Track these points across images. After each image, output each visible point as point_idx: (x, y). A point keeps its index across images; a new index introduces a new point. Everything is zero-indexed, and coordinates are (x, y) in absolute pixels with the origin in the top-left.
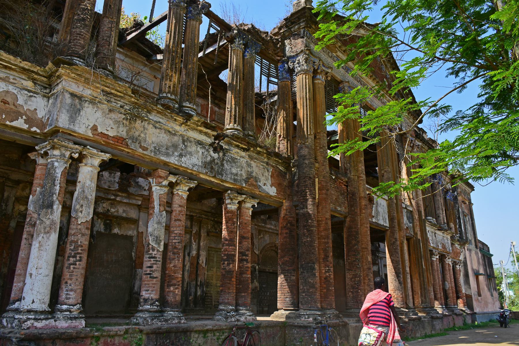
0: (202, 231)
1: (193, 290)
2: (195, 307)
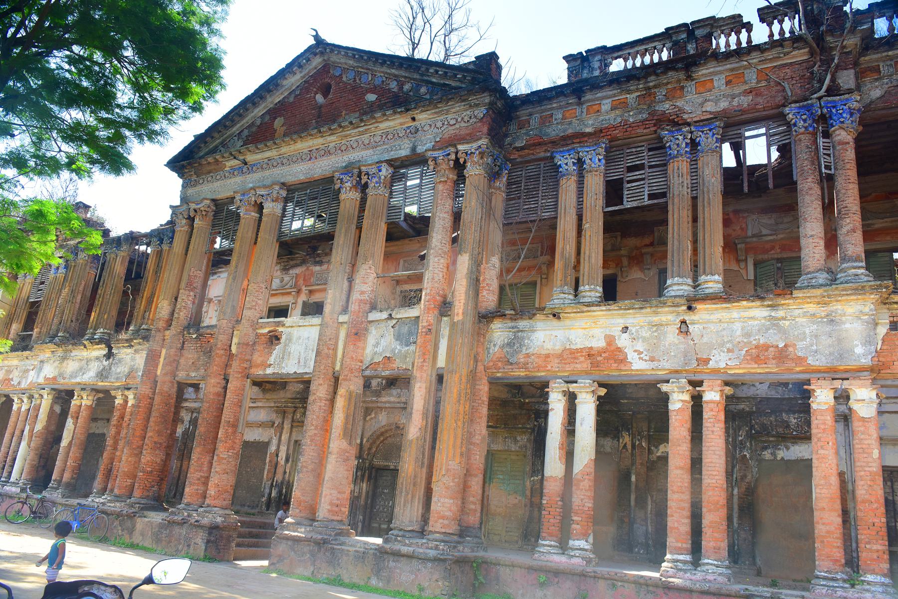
1: (267, 491)
2: (268, 510)
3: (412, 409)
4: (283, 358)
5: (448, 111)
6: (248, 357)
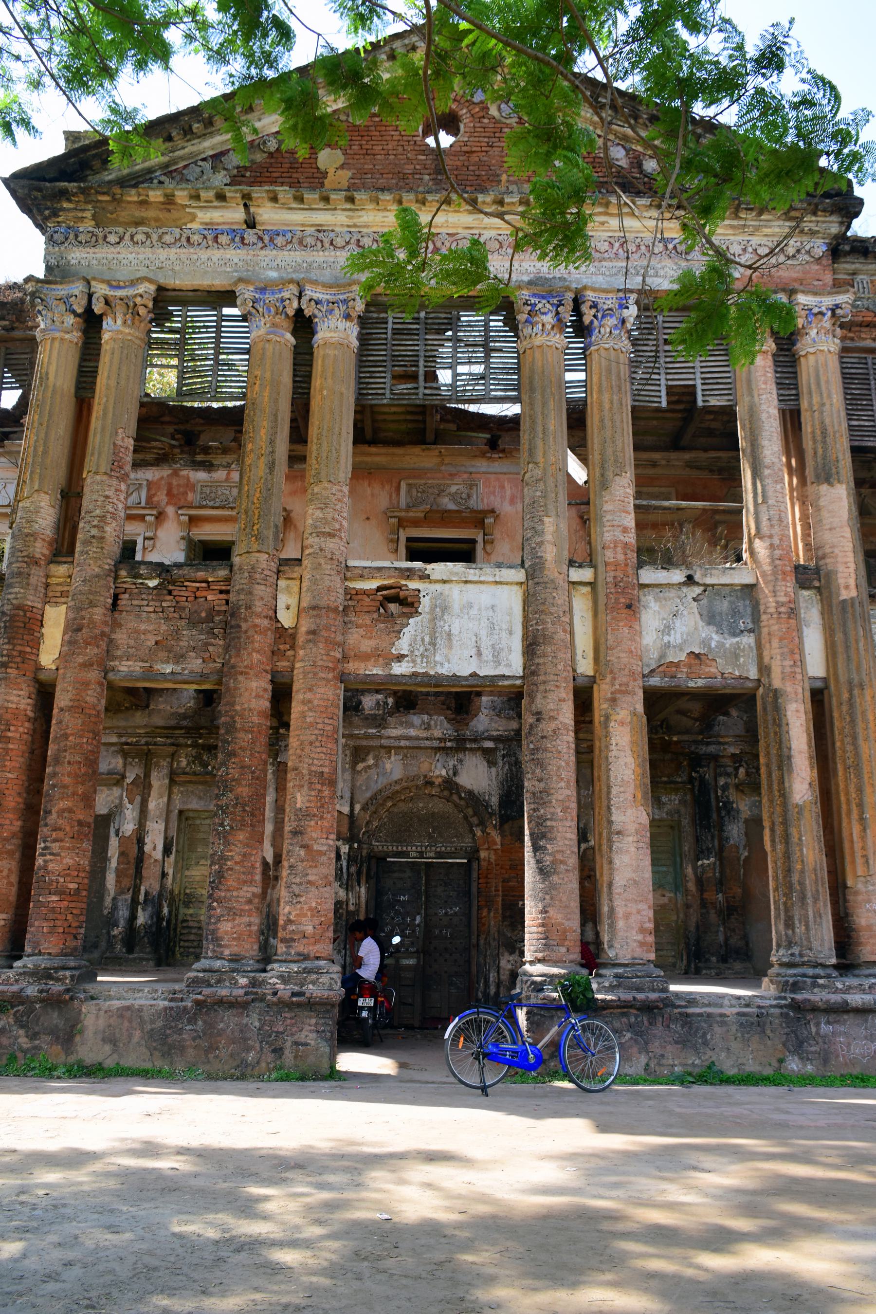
0: (154, 774)
1: (123, 913)
2: (130, 950)
3: (790, 749)
4: (433, 644)
5: (757, 229)
6: (339, 638)
